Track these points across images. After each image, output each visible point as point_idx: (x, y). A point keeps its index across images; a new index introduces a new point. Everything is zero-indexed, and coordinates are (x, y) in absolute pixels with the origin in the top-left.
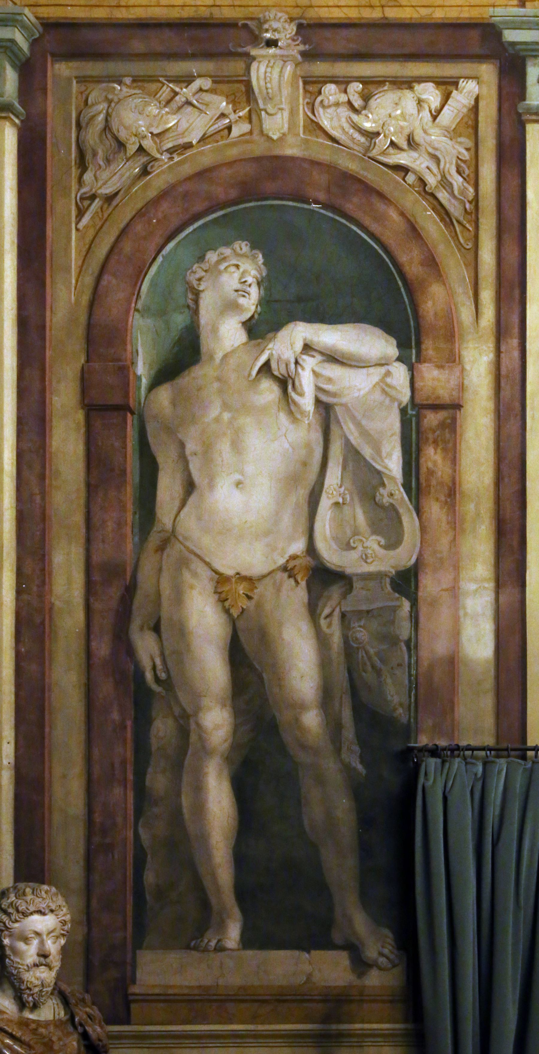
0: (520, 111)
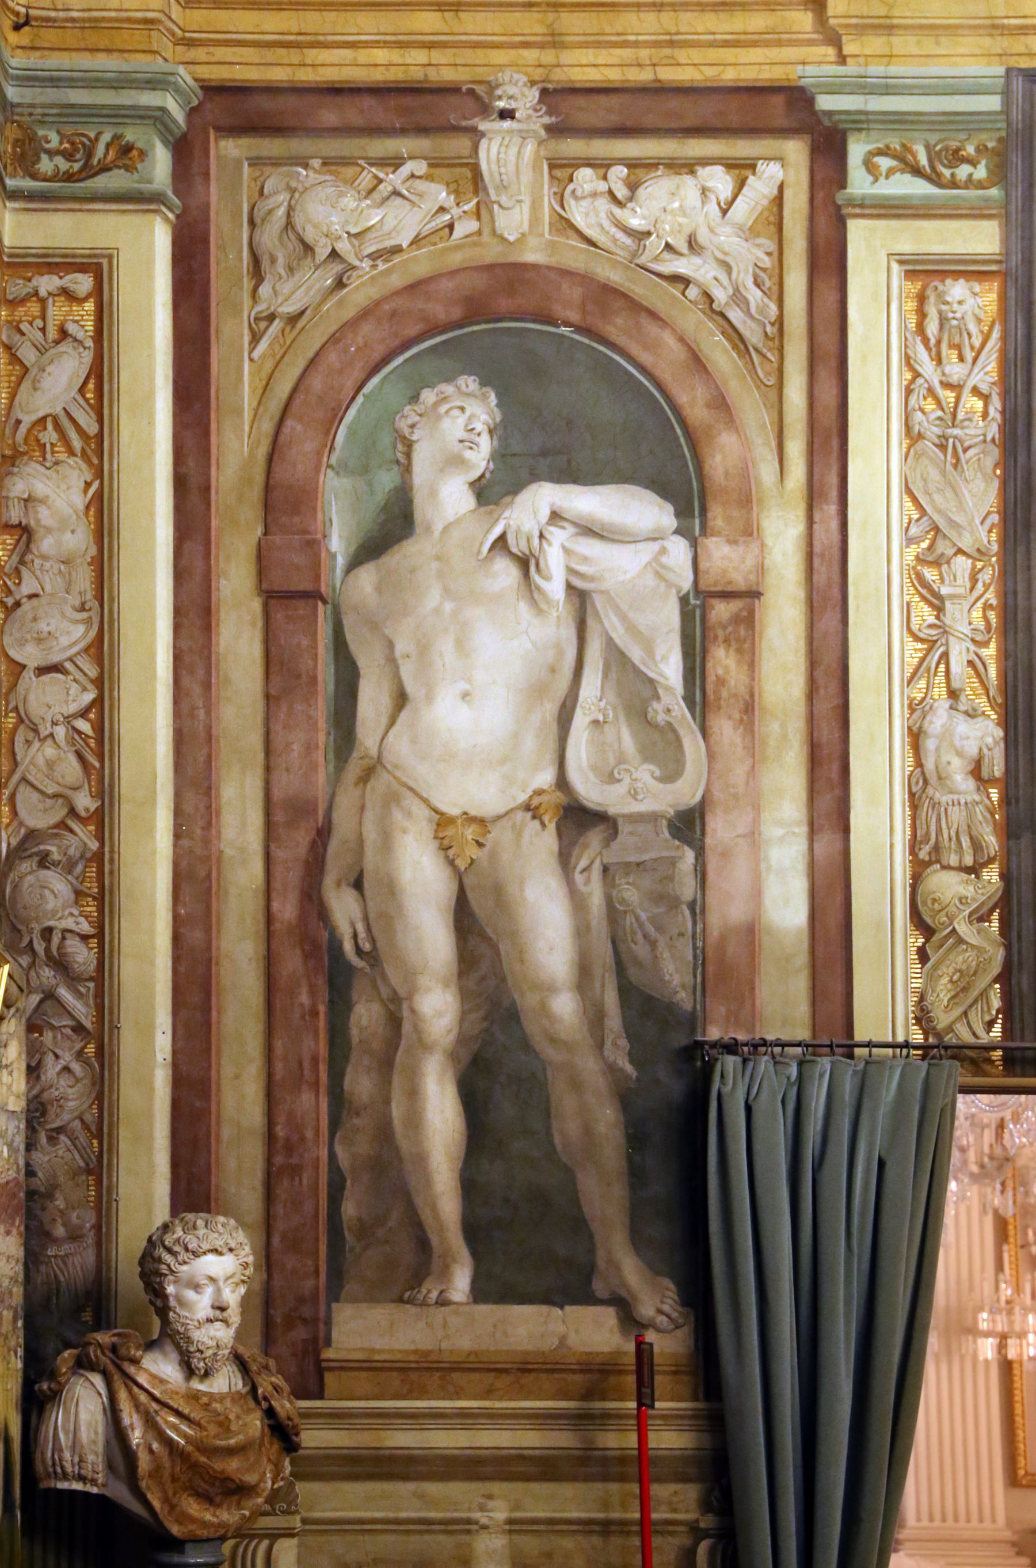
0: (840, 202)
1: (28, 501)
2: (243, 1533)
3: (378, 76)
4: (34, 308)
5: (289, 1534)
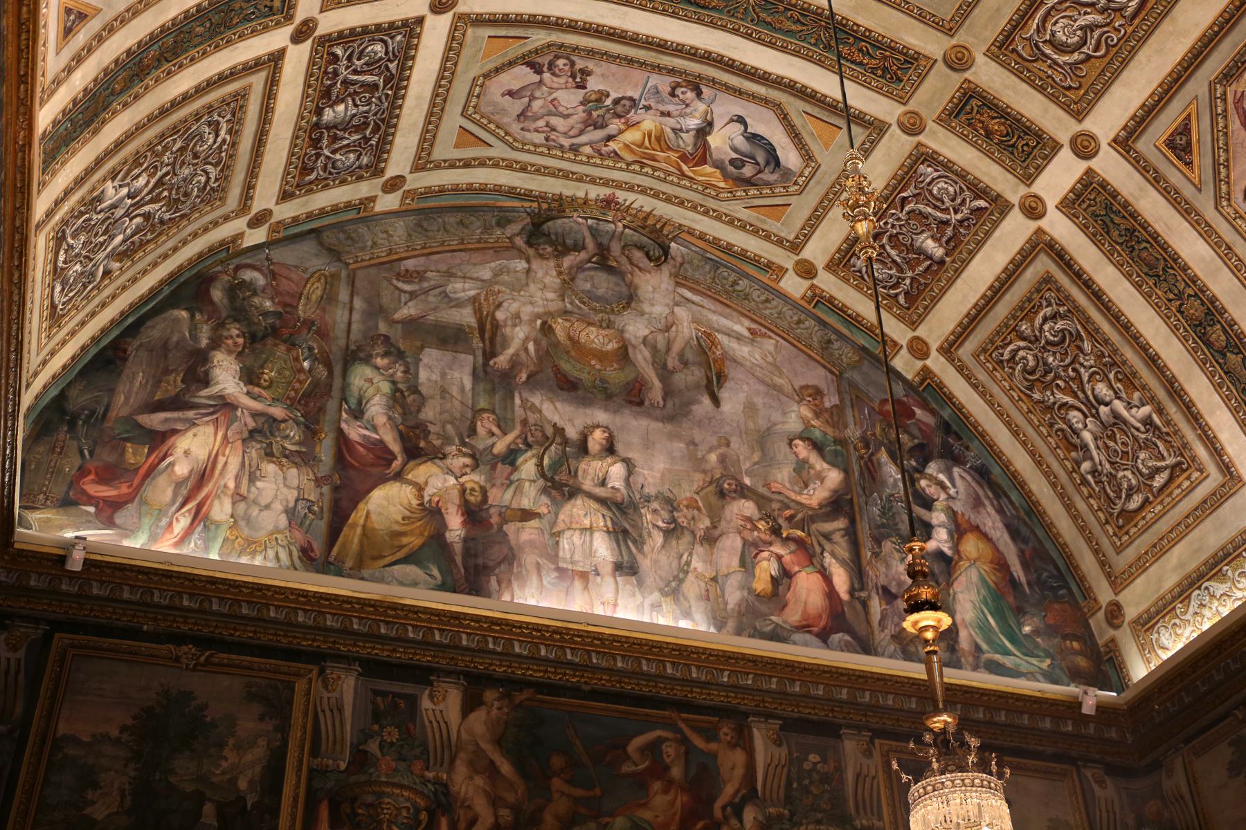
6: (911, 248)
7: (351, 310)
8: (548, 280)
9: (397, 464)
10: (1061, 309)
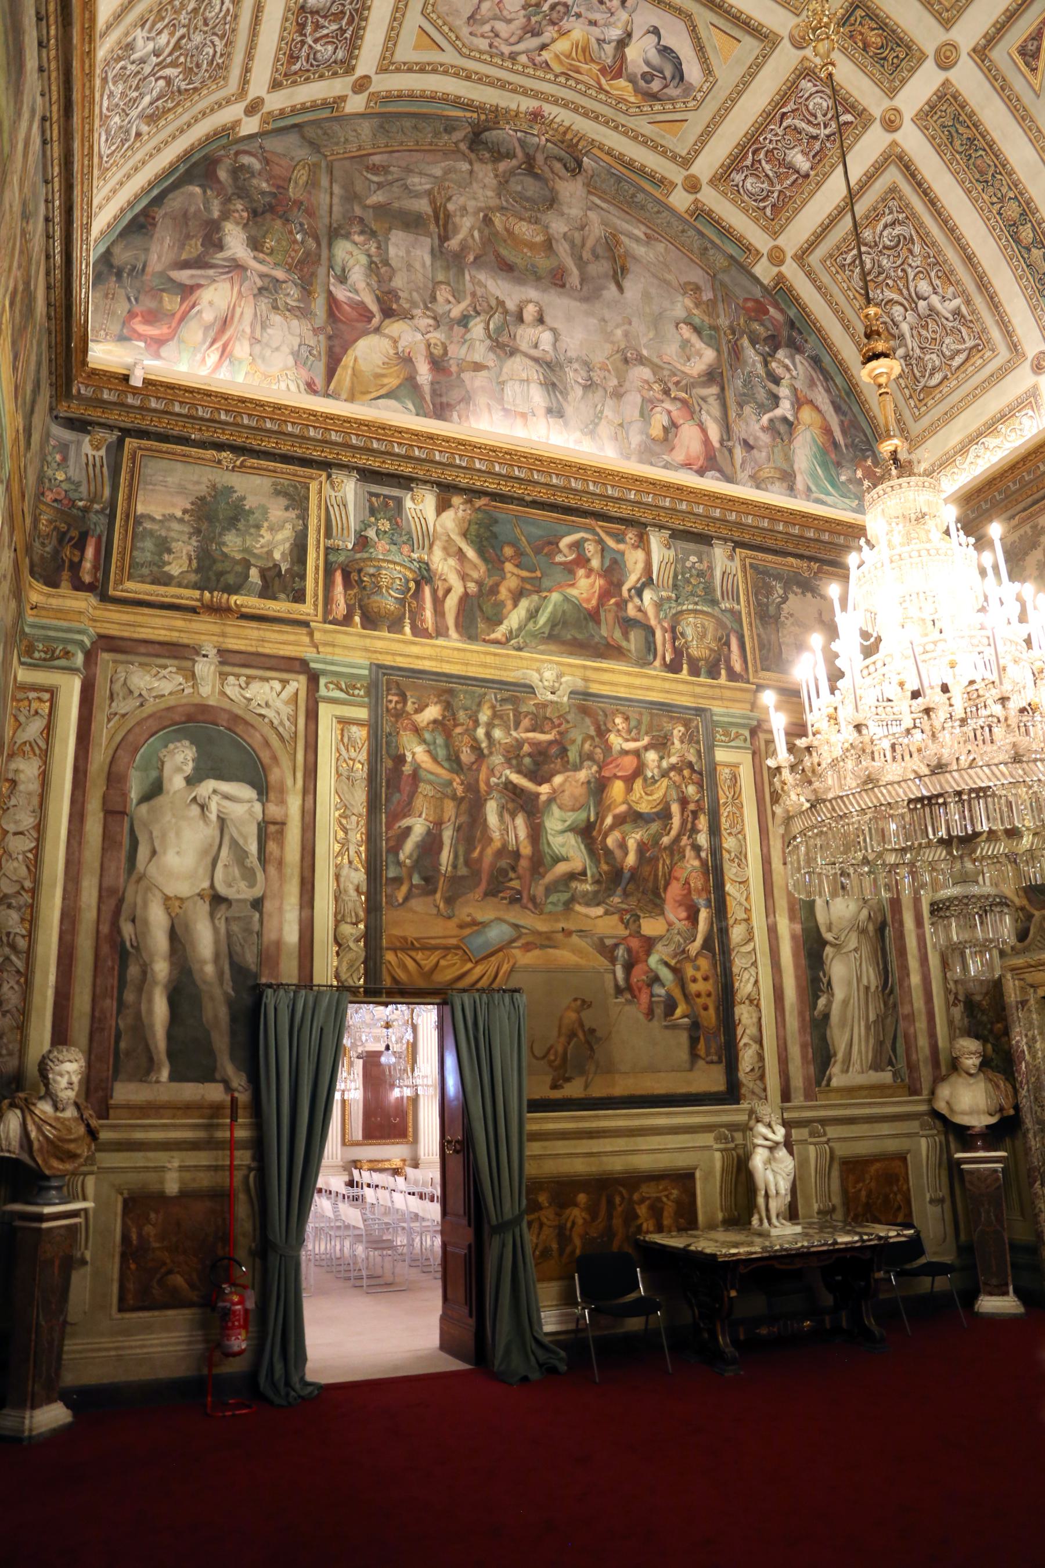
1: (16, 771)
2: (74, 1173)
3: (161, 639)
4: (26, 703)
5: (91, 1173)
6: (782, 163)
7: (331, 194)
8: (487, 181)
9: (376, 321)
10: (901, 216)
